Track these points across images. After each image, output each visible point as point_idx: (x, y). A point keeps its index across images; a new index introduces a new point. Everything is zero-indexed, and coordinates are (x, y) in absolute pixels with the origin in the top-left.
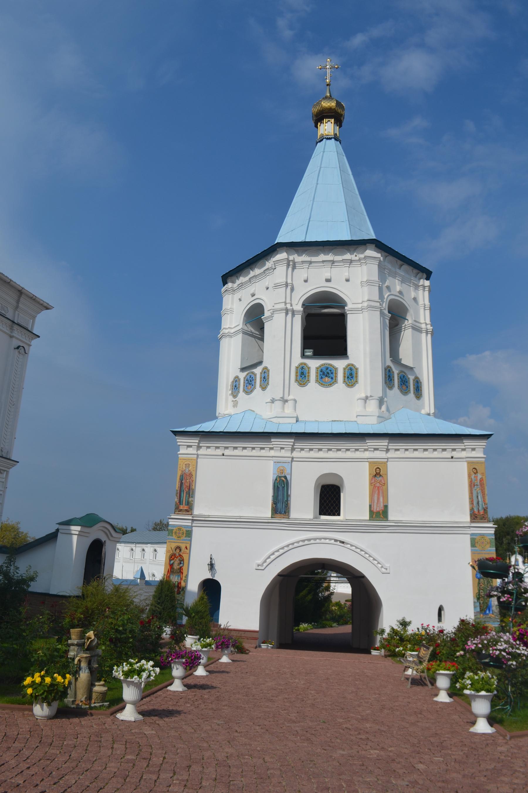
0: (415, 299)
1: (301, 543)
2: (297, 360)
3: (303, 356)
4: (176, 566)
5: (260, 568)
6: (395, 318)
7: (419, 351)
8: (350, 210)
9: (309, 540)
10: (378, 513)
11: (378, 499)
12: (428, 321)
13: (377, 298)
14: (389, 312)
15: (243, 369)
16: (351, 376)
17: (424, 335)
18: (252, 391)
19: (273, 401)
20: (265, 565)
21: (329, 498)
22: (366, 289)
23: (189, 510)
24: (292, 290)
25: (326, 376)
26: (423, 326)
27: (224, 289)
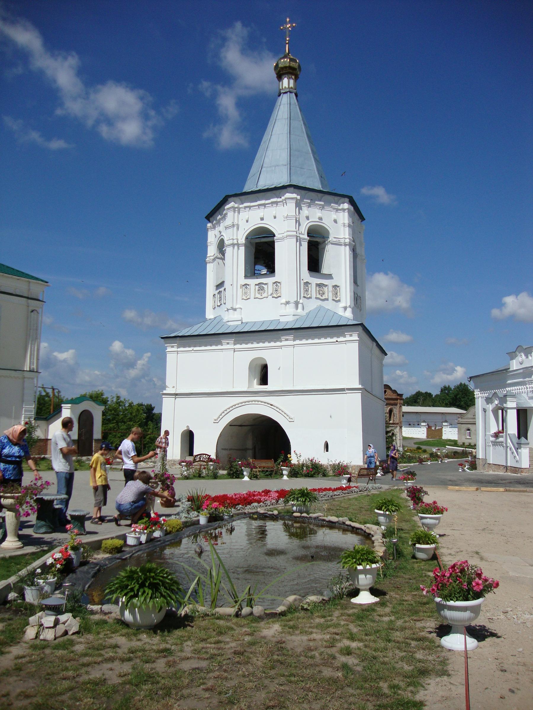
1: (240, 405)
3: (246, 277)
5: (216, 422)
9: (245, 402)
12: (347, 236)
14: (308, 236)
20: (219, 419)
24: (238, 229)
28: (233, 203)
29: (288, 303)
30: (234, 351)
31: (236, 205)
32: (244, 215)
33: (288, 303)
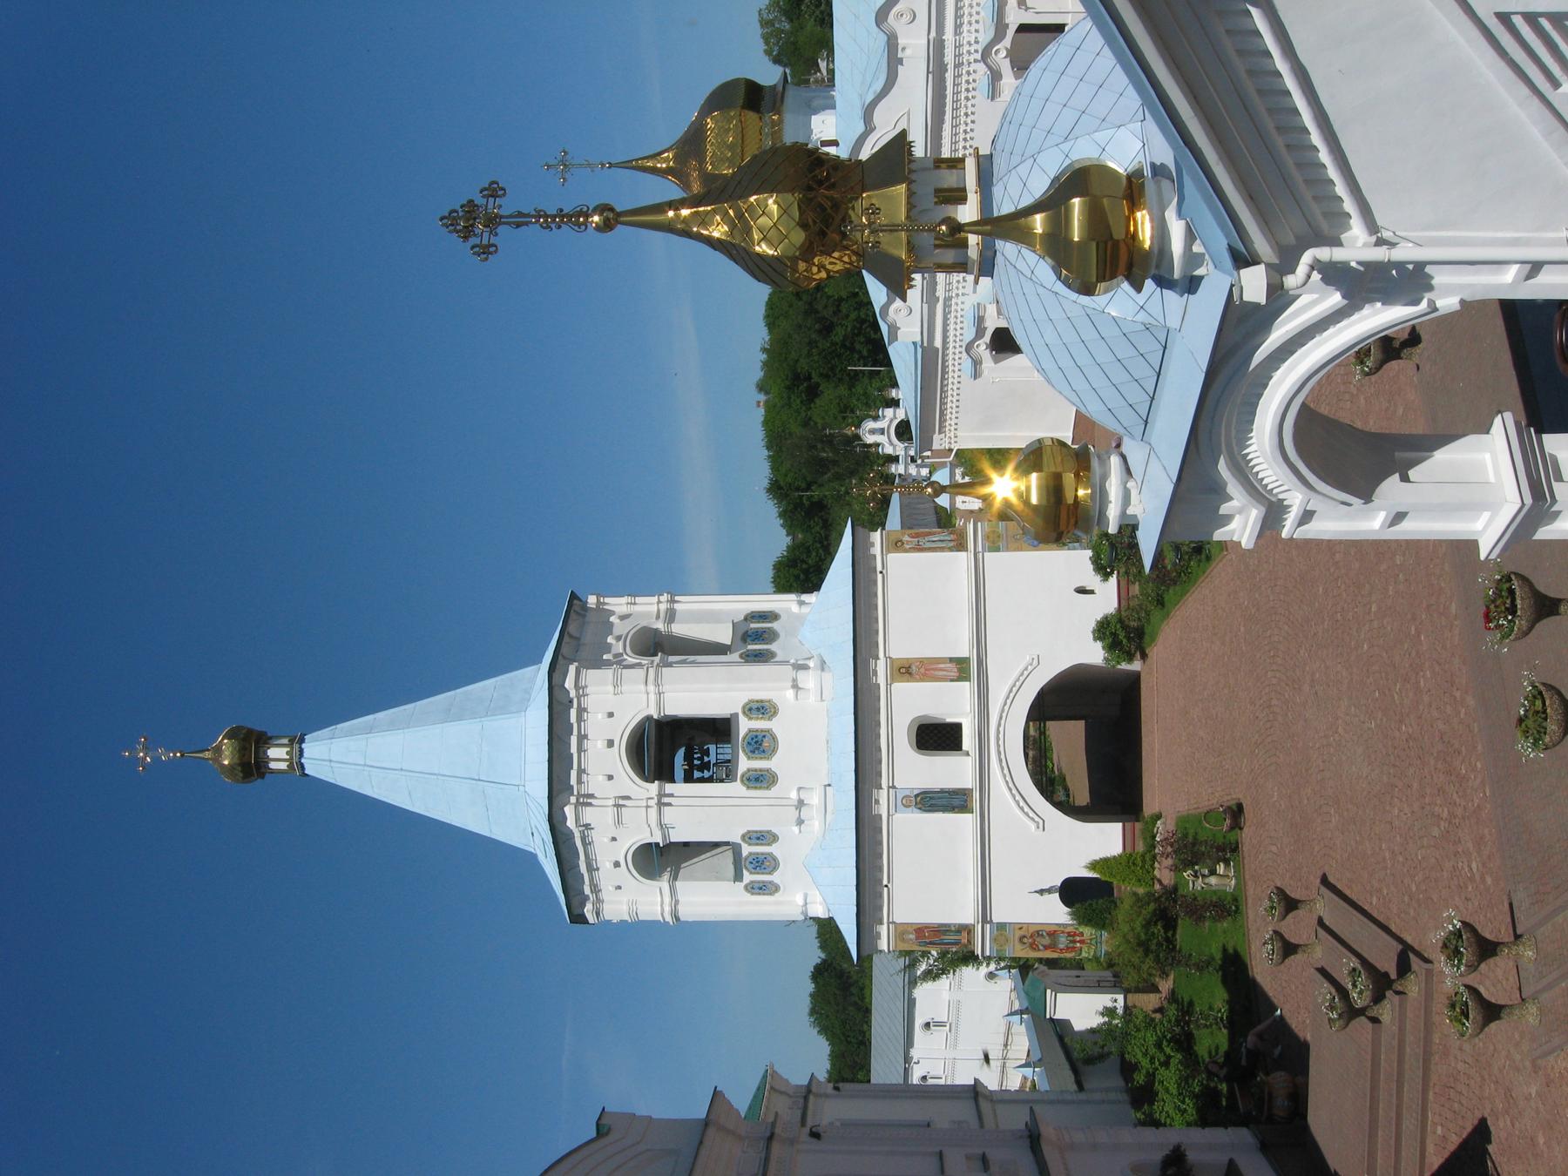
0: (623, 618)
2: (735, 788)
3: (729, 777)
4: (1047, 941)
6: (658, 646)
7: (709, 614)
8: (450, 716)
10: (960, 670)
12: (655, 599)
13: (640, 673)
14: (655, 655)
15: (738, 877)
16: (761, 709)
17: (676, 606)
18: (775, 859)
19: (800, 822)
21: (937, 737)
23: (967, 929)
24: (628, 798)
25: (760, 744)
26: (663, 607)
27: (591, 918)
28: (567, 809)
29: (795, 686)
30: (894, 787)
31: (573, 799)
32: (594, 783)
33: (795, 686)
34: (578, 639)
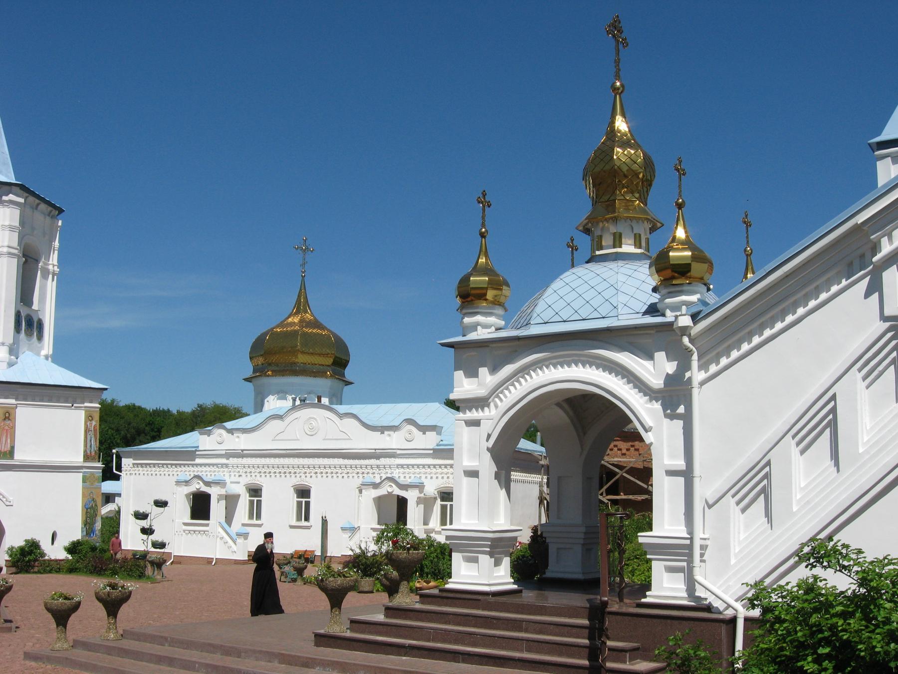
11: (6, 440)
22: (7, 233)
34: (36, 208)
